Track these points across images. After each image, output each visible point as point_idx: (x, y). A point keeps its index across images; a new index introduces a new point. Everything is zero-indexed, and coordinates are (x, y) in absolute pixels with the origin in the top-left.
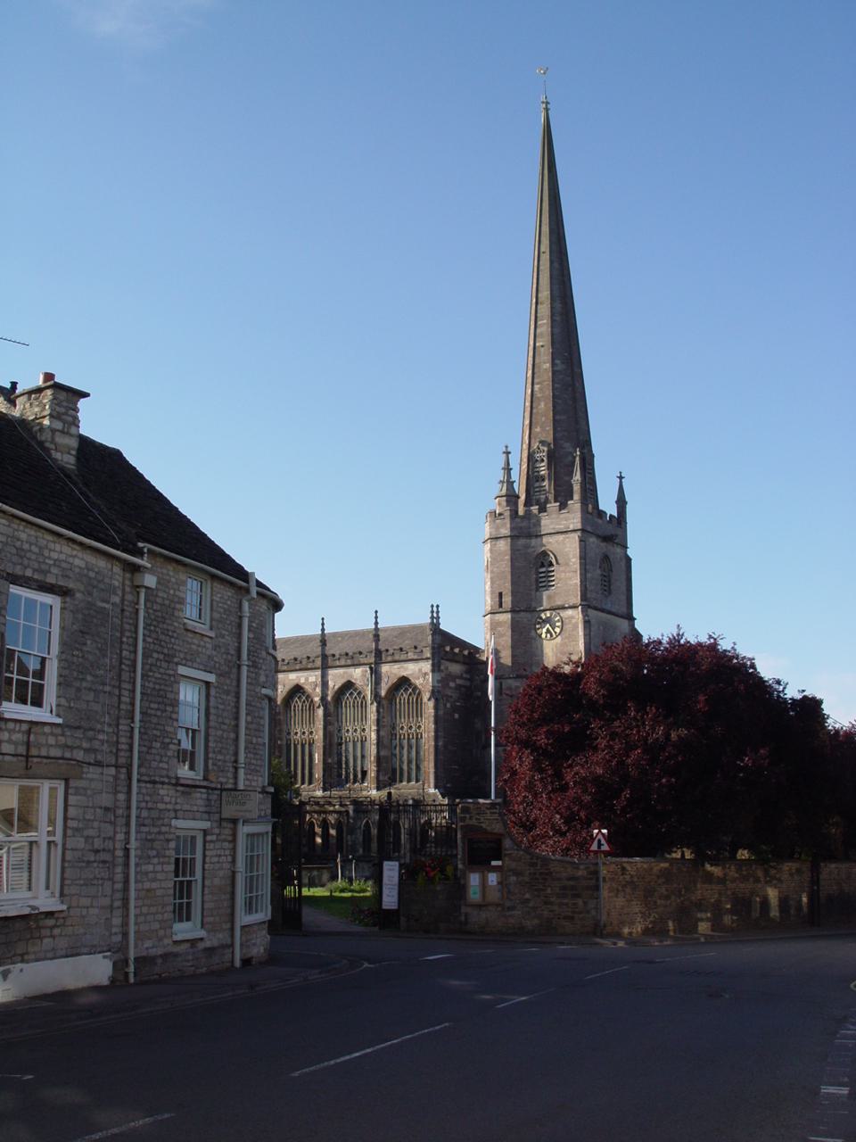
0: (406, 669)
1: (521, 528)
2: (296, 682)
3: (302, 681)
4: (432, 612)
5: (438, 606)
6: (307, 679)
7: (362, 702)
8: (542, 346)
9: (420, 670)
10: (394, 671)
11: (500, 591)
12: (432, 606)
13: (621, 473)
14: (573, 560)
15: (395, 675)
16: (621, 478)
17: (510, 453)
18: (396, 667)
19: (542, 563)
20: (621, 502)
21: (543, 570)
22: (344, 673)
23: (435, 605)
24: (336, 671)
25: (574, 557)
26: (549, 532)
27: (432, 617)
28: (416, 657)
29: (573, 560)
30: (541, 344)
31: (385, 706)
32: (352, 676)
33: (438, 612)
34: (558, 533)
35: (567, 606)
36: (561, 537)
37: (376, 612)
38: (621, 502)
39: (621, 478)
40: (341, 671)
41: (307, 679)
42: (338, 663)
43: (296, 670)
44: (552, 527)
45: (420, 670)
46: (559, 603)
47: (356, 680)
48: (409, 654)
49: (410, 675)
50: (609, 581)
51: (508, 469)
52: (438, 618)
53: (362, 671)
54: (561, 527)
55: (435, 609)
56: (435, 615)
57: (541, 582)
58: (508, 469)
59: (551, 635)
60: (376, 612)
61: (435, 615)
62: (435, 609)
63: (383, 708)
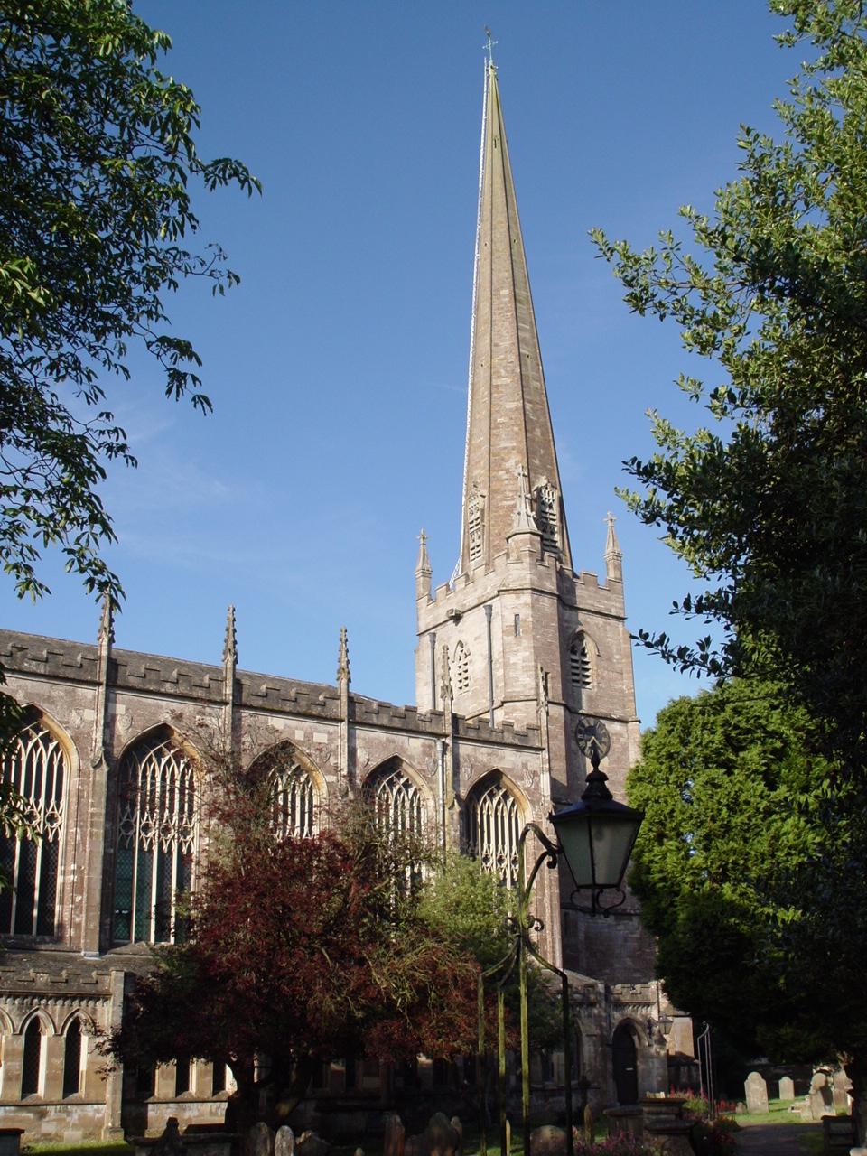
0: (502, 758)
2: (284, 736)
6: (309, 736)
9: (525, 766)
10: (485, 759)
22: (388, 740)
26: (587, 607)
28: (517, 742)
36: (601, 620)
40: (383, 736)
41: (309, 736)
42: (375, 721)
44: (589, 602)
45: (525, 766)
48: (506, 734)
53: (423, 745)
54: (601, 607)
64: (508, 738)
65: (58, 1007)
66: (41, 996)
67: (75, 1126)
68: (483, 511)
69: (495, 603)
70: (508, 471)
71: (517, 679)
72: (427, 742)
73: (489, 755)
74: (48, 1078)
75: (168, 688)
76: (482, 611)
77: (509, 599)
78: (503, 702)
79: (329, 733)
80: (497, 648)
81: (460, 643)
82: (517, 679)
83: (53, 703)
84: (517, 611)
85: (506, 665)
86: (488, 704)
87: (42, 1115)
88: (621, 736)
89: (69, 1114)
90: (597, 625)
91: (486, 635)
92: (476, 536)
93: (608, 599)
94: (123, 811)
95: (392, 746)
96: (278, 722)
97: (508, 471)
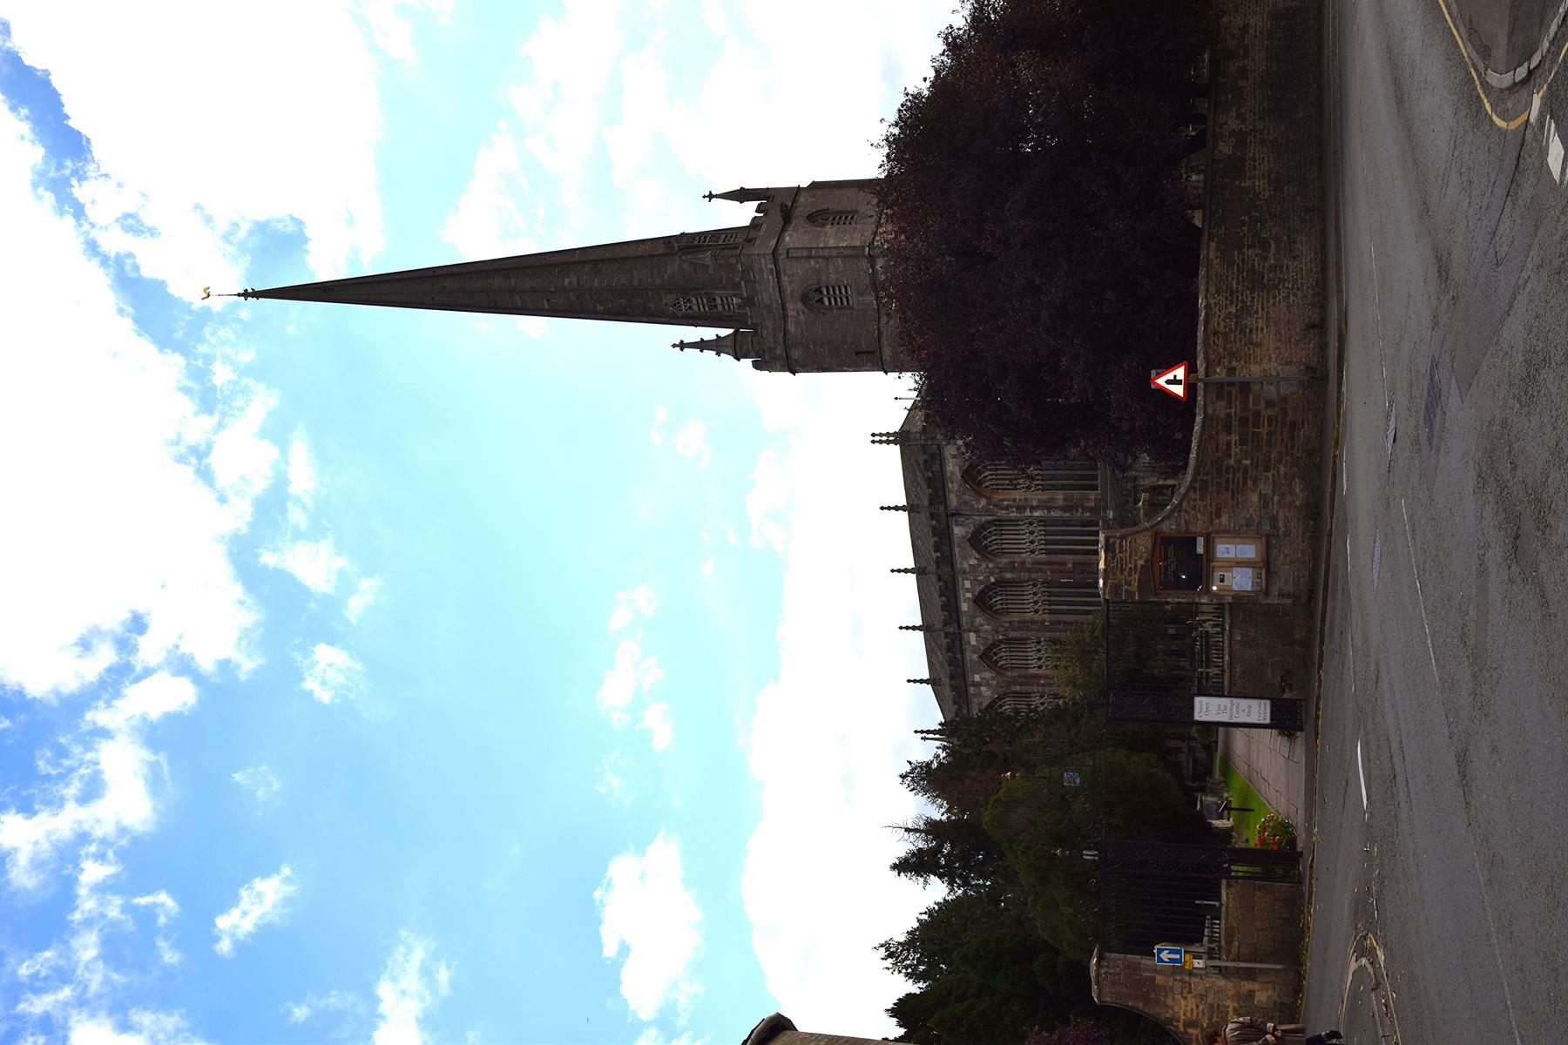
1: (774, 329)
2: (971, 603)
3: (969, 595)
4: (881, 442)
5: (873, 435)
6: (968, 590)
7: (996, 525)
8: (548, 300)
10: (956, 487)
11: (854, 354)
12: (873, 442)
13: (704, 197)
14: (813, 263)
16: (711, 196)
17: (682, 341)
18: (950, 485)
19: (818, 301)
20: (741, 195)
21: (826, 300)
23: (873, 438)
24: (957, 556)
25: (810, 263)
26: (778, 294)
27: (888, 442)
28: (938, 462)
29: (813, 263)
30: (545, 302)
31: (1001, 498)
32: (962, 538)
33: (881, 435)
34: (779, 283)
35: (871, 271)
36: (785, 279)
37: (882, 508)
38: (741, 195)
39: (711, 196)
40: (957, 550)
41: (968, 590)
42: (948, 554)
43: (957, 602)
45: (954, 457)
47: (967, 532)
48: (934, 470)
49: (959, 468)
50: (841, 212)
51: (702, 345)
52: (888, 434)
53: (957, 525)
55: (877, 438)
56: (884, 438)
57: (842, 304)
58: (702, 345)
60: (882, 508)
61: (884, 438)
62: (877, 438)
63: (1003, 500)
72: (954, 523)
73: (952, 482)
75: (958, 656)
79: (963, 580)
90: (791, 283)
96: (964, 607)
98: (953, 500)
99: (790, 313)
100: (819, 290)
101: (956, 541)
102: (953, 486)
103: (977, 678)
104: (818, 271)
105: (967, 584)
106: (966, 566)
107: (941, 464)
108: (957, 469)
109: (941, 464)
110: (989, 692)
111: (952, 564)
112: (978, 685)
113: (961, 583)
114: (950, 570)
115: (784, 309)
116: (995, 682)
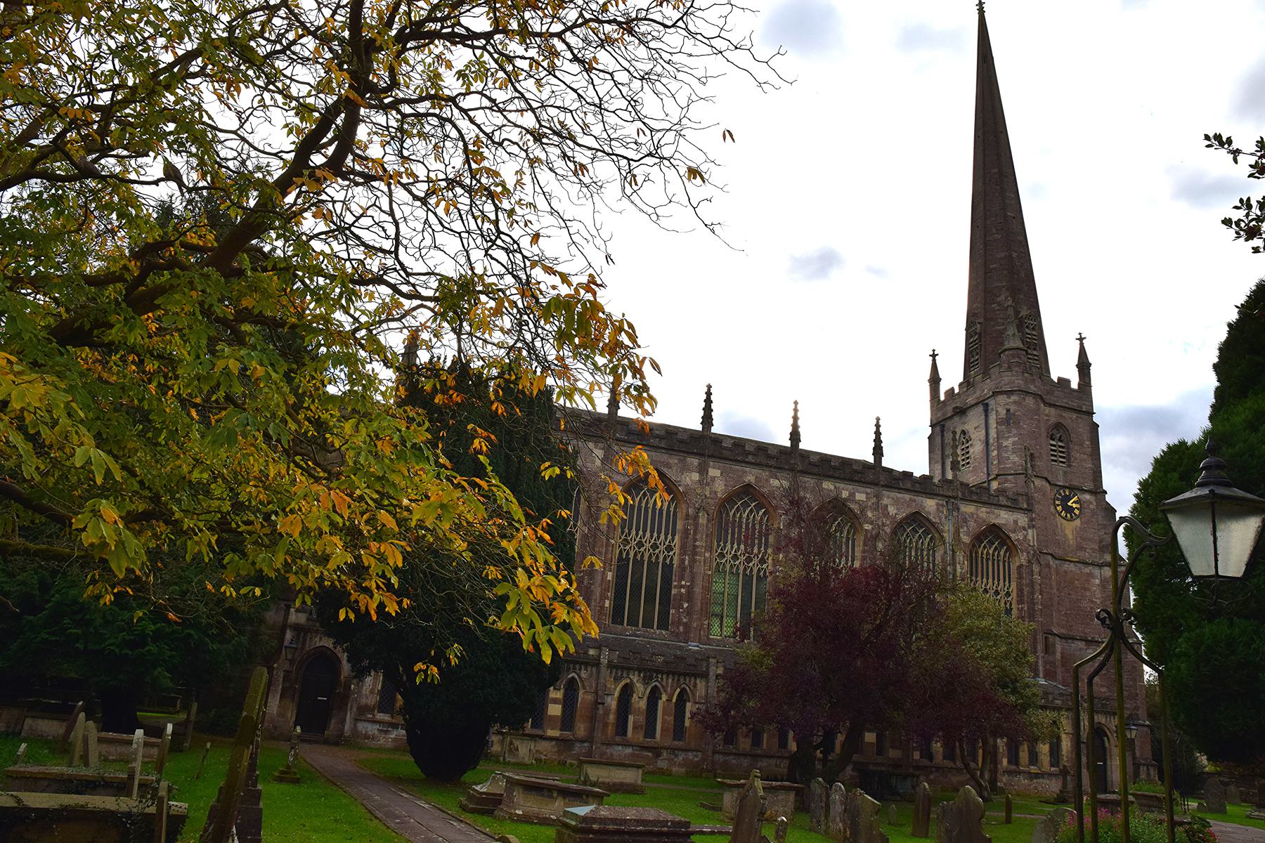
2: (833, 495)
3: (845, 494)
9: (1016, 522)
10: (983, 515)
15: (984, 521)
18: (984, 509)
24: (899, 495)
36: (1074, 416)
40: (907, 497)
41: (852, 495)
45: (1016, 522)
46: (1075, 483)
53: (937, 504)
59: (1071, 517)
64: (1003, 501)
65: (670, 680)
66: (657, 672)
67: (680, 765)
68: (980, 334)
69: (992, 402)
70: (999, 304)
71: (1008, 458)
72: (940, 502)
74: (662, 730)
75: (750, 458)
76: (981, 408)
77: (1002, 399)
78: (998, 475)
79: (867, 494)
80: (993, 433)
81: (963, 432)
82: (1008, 458)
83: (670, 468)
84: (1008, 407)
85: (999, 447)
86: (985, 476)
87: (658, 755)
88: (1091, 503)
89: (676, 756)
91: (983, 426)
92: (974, 353)
93: (1080, 399)
94: (719, 545)
95: (914, 504)
96: (828, 485)
97: (999, 304)
98: (968, 509)
99: (1047, 410)
100: (1060, 440)
101: (919, 499)
102: (983, 512)
103: (714, 472)
104: (1081, 445)
105: (860, 497)
106: (885, 501)
107: (1008, 507)
108: (1003, 522)
109: (1008, 507)
110: (690, 483)
111: (888, 487)
112: (703, 470)
113: (861, 489)
114: (882, 483)
115: (1051, 405)
116: (707, 493)
